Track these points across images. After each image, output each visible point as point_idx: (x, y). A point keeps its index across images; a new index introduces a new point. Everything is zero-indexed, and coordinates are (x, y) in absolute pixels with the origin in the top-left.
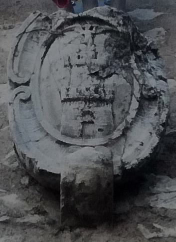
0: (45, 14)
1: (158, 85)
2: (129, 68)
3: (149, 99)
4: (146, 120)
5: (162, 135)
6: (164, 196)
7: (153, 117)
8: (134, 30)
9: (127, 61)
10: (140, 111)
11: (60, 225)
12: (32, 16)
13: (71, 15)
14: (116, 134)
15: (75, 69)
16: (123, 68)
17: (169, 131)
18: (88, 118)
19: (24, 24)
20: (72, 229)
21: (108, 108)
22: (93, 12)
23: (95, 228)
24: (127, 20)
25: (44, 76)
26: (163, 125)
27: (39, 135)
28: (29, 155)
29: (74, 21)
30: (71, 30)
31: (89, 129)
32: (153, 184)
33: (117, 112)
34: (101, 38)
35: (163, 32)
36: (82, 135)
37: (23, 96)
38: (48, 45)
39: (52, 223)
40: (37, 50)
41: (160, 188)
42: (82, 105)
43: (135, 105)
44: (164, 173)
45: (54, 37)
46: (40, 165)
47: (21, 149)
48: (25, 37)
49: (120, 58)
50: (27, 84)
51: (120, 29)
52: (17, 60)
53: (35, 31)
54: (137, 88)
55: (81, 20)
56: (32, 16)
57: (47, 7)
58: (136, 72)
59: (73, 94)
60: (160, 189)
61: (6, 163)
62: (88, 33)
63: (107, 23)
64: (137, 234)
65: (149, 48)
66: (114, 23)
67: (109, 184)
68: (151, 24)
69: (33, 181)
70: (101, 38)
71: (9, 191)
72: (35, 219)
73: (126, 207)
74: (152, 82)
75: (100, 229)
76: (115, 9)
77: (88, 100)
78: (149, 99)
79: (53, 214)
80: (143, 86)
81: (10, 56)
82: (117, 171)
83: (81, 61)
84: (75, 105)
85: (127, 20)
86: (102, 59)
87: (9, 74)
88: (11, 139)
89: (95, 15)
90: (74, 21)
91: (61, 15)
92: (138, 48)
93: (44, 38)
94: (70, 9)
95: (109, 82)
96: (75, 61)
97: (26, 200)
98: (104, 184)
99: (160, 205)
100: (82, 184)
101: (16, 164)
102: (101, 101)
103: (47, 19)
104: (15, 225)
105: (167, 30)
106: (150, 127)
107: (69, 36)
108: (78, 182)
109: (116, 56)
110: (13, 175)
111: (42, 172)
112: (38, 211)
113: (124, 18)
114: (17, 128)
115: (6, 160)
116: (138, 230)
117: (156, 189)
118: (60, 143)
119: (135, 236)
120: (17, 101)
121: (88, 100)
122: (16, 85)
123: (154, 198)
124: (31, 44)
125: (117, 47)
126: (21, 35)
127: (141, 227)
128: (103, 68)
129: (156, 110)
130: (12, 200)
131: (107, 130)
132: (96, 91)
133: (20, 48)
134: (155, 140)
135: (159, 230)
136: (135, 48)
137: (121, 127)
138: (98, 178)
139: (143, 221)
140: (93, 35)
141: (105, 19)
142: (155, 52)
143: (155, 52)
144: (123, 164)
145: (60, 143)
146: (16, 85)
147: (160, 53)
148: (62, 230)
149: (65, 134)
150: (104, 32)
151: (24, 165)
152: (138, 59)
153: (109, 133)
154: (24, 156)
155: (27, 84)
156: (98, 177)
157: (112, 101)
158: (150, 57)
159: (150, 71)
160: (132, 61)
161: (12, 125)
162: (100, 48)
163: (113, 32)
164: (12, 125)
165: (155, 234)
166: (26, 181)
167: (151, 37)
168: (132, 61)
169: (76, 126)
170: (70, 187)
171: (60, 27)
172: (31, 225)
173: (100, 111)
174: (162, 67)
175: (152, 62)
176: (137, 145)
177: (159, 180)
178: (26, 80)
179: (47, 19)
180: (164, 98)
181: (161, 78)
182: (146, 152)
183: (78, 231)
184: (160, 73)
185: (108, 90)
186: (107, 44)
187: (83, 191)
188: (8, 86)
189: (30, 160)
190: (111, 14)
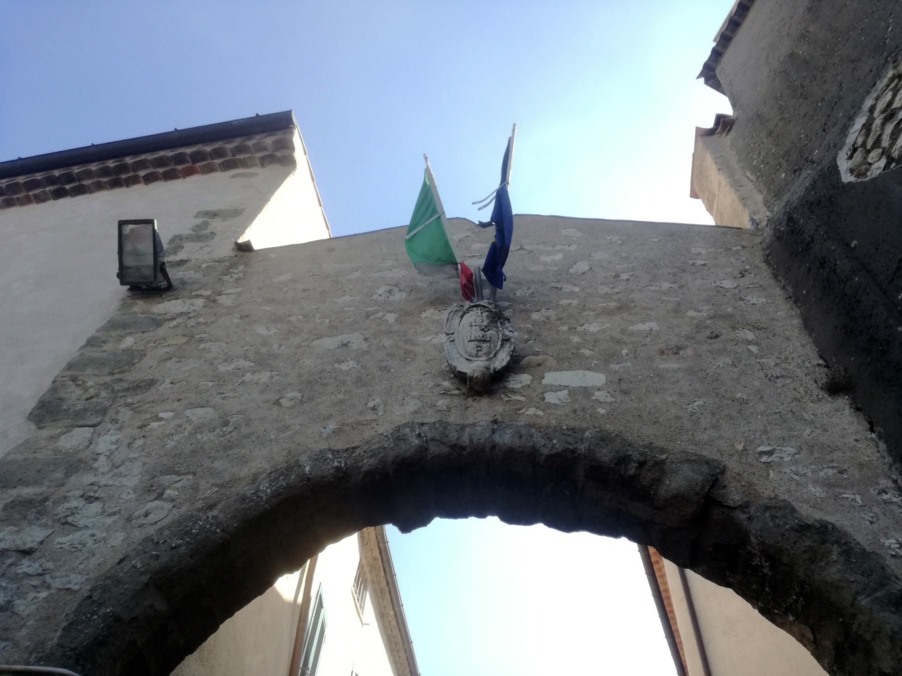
0: (460, 304)
1: (510, 334)
2: (497, 327)
3: (506, 340)
4: (505, 349)
5: (511, 356)
6: (512, 382)
7: (508, 348)
8: (499, 311)
9: (497, 324)
10: (502, 346)
11: (467, 395)
12: (455, 305)
13: (472, 304)
14: (492, 356)
15: (474, 327)
16: (494, 327)
17: (515, 354)
18: (479, 349)
19: (452, 308)
20: (472, 396)
21: (488, 344)
22: (482, 303)
23: (482, 396)
24: (496, 306)
25: (460, 330)
26: (512, 351)
27: (458, 356)
28: (454, 365)
29: (473, 306)
30: (472, 310)
31: (480, 353)
32: (508, 377)
33: (492, 346)
34: (485, 314)
35: (512, 311)
36: (477, 356)
37: (451, 339)
38: (462, 317)
39: (464, 394)
40: (457, 319)
41: (510, 379)
42: (477, 343)
43: (500, 343)
44: (512, 372)
45: (465, 313)
46: (459, 369)
47: (450, 362)
48: (452, 314)
49: (493, 323)
50: (453, 334)
51: (493, 310)
52: (448, 323)
53: (457, 311)
54: (500, 335)
55: (476, 306)
56: (455, 305)
57: (462, 301)
58: (500, 328)
59: (473, 338)
60: (511, 379)
61: (444, 368)
62: (479, 312)
63: (487, 307)
64: (501, 399)
65: (506, 318)
66: (491, 308)
67: (488, 377)
68: (507, 308)
69: (455, 376)
70: (485, 314)
71: (445, 380)
72: (457, 392)
73: (496, 387)
74: (507, 333)
75: (484, 396)
76: (491, 301)
77: (479, 341)
78: (506, 340)
79: (464, 390)
80: (503, 335)
81: (446, 322)
82: (492, 371)
83: (476, 324)
84: (474, 343)
85: (496, 306)
86: (485, 323)
87: (445, 329)
88: (446, 358)
89: (482, 304)
90: (473, 306)
91: (467, 304)
92: (501, 318)
93: (460, 314)
94: (472, 301)
95: (488, 333)
96: (473, 324)
97: (452, 384)
98: (486, 378)
99: (511, 386)
100: (477, 377)
101: (448, 368)
102: (485, 341)
103: (461, 306)
104: (448, 395)
105: (514, 310)
106: (506, 353)
107: (471, 313)
108: (475, 376)
109: (492, 322)
110: (447, 373)
111: (459, 372)
112: (458, 389)
113: (495, 305)
114: (448, 353)
115: (444, 366)
116: (501, 397)
117: (509, 379)
118: (467, 359)
119: (499, 399)
120: (448, 341)
121: (479, 341)
122: (448, 334)
123: (508, 383)
124: (455, 316)
125: (492, 318)
126: (450, 312)
127: (502, 396)
128: (486, 327)
129: (509, 345)
130: (446, 384)
131: (488, 354)
132: (483, 337)
133: (450, 318)
134: (509, 358)
135: (510, 397)
136: (500, 318)
137: (494, 352)
138: (484, 374)
139: (505, 393)
140: (482, 313)
141: (487, 306)
142: (508, 320)
143: (508, 320)
144: (495, 368)
145: (467, 359)
146: (448, 334)
147: (511, 320)
148: (468, 397)
149: (469, 355)
150: (486, 311)
151: (452, 369)
152: (501, 323)
153: (489, 355)
154: (451, 365)
155: (453, 334)
156: (484, 374)
157: (489, 341)
158: (506, 322)
159: (506, 328)
160: (499, 324)
161: (446, 351)
162: (485, 318)
163: (490, 311)
164: (446, 351)
165: (508, 399)
166: (452, 376)
167: (507, 314)
168: (499, 324)
169: (474, 352)
170: (471, 378)
171: (467, 309)
172: (455, 395)
173: (485, 346)
174: (512, 326)
175: (507, 325)
176: (501, 360)
177: (510, 375)
178: (452, 332)
179: (461, 306)
180: (513, 340)
181: (511, 331)
182: (504, 363)
183: (475, 397)
184: (511, 329)
185: (488, 336)
186: (488, 317)
187: (477, 380)
188: (444, 335)
189: (454, 367)
190: (489, 303)
